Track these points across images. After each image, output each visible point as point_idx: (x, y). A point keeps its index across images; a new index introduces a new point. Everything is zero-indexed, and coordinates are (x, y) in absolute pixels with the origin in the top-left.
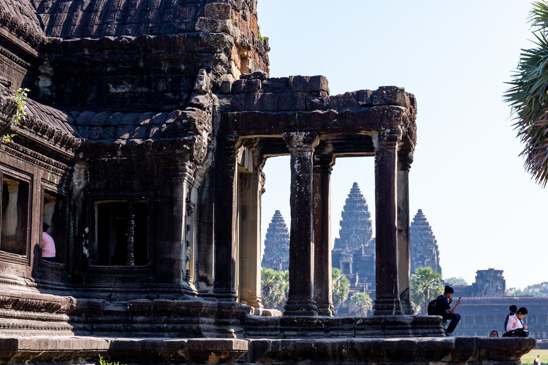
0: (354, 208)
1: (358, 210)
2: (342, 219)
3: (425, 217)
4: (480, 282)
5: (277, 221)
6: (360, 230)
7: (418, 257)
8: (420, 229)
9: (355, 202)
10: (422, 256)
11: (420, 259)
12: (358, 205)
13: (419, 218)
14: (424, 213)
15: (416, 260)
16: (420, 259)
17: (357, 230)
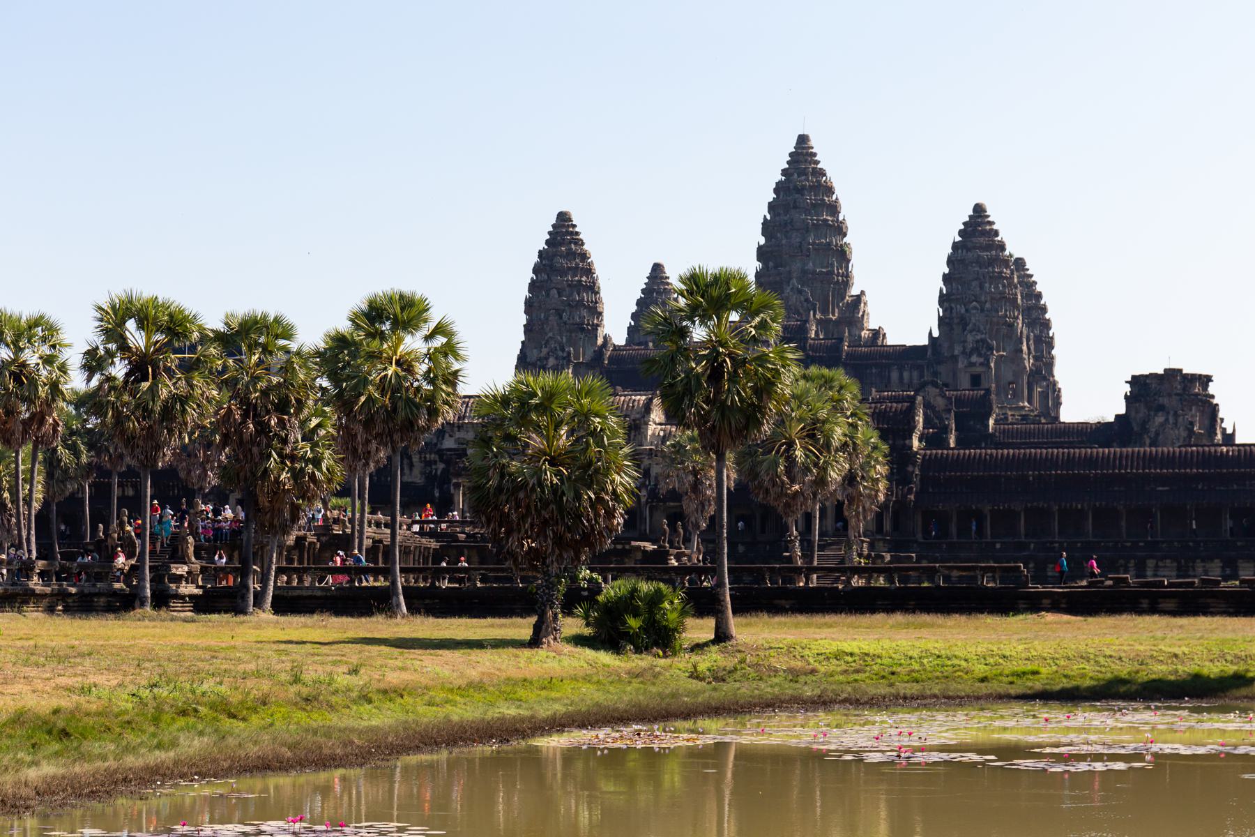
0: (795, 207)
1: (807, 212)
2: (762, 241)
3: (995, 227)
4: (1137, 412)
5: (561, 244)
6: (814, 273)
7: (970, 346)
8: (978, 261)
9: (800, 191)
10: (983, 341)
11: (975, 350)
12: (809, 198)
13: (975, 230)
14: (993, 214)
15: (964, 353)
16: (975, 350)
17: (804, 272)
